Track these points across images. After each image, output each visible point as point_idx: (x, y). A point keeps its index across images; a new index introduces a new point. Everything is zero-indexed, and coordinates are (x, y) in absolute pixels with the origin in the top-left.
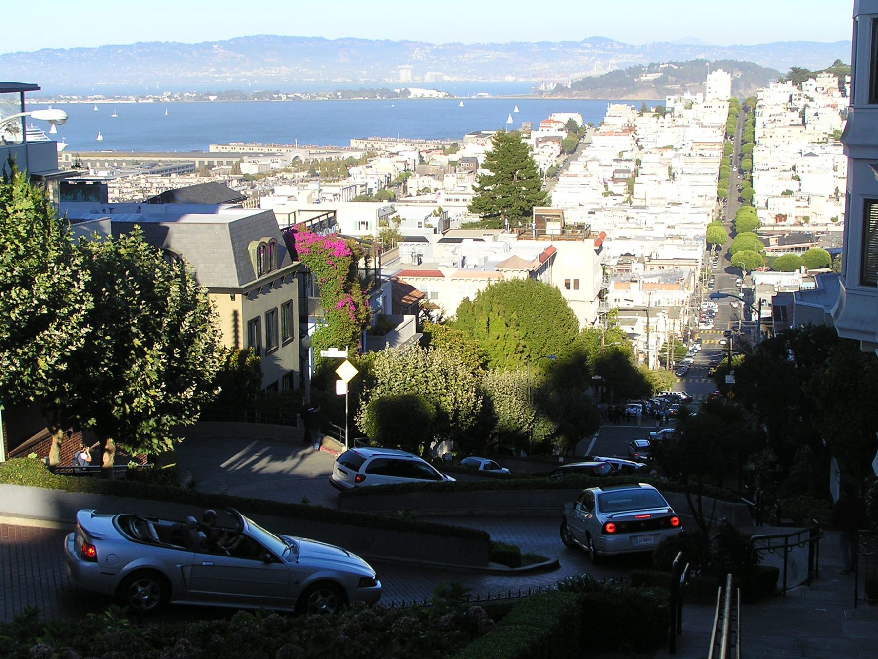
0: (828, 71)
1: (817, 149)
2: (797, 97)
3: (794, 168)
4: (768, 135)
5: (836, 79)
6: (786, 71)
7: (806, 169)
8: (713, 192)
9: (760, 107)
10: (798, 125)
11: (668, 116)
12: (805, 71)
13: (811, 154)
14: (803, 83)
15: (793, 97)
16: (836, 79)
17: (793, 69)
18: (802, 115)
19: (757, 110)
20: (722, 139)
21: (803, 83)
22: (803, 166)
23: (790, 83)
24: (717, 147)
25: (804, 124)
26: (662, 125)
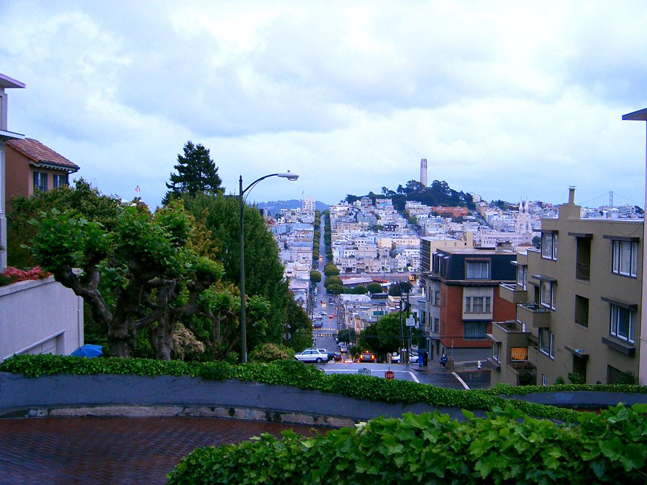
0: (366, 196)
1: (366, 233)
2: (351, 209)
3: (353, 243)
4: (338, 227)
5: (371, 200)
6: (344, 198)
7: (361, 243)
8: (310, 256)
9: (333, 214)
10: (354, 222)
11: (283, 218)
12: (355, 197)
13: (363, 236)
14: (354, 203)
15: (350, 209)
16: (371, 200)
17: (348, 195)
18: (355, 217)
19: (331, 216)
20: (313, 230)
21: (354, 203)
22: (359, 242)
23: (347, 202)
24: (311, 233)
25: (357, 221)
26: (280, 222)
